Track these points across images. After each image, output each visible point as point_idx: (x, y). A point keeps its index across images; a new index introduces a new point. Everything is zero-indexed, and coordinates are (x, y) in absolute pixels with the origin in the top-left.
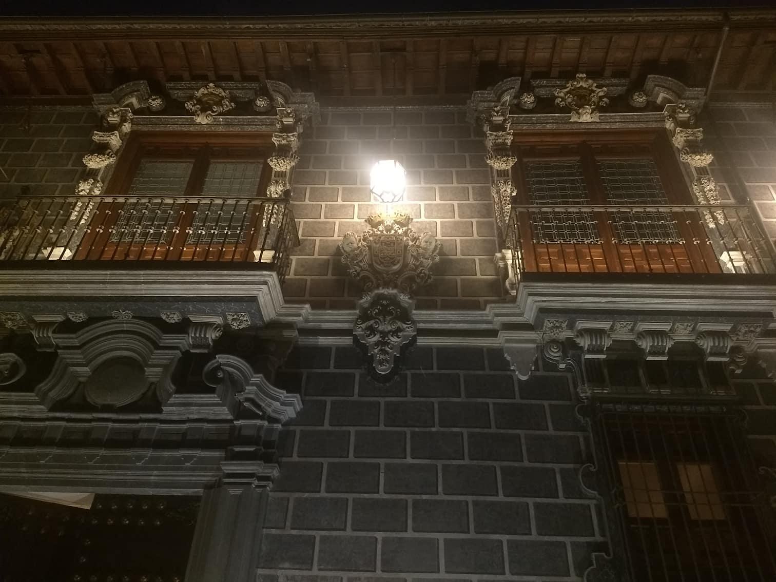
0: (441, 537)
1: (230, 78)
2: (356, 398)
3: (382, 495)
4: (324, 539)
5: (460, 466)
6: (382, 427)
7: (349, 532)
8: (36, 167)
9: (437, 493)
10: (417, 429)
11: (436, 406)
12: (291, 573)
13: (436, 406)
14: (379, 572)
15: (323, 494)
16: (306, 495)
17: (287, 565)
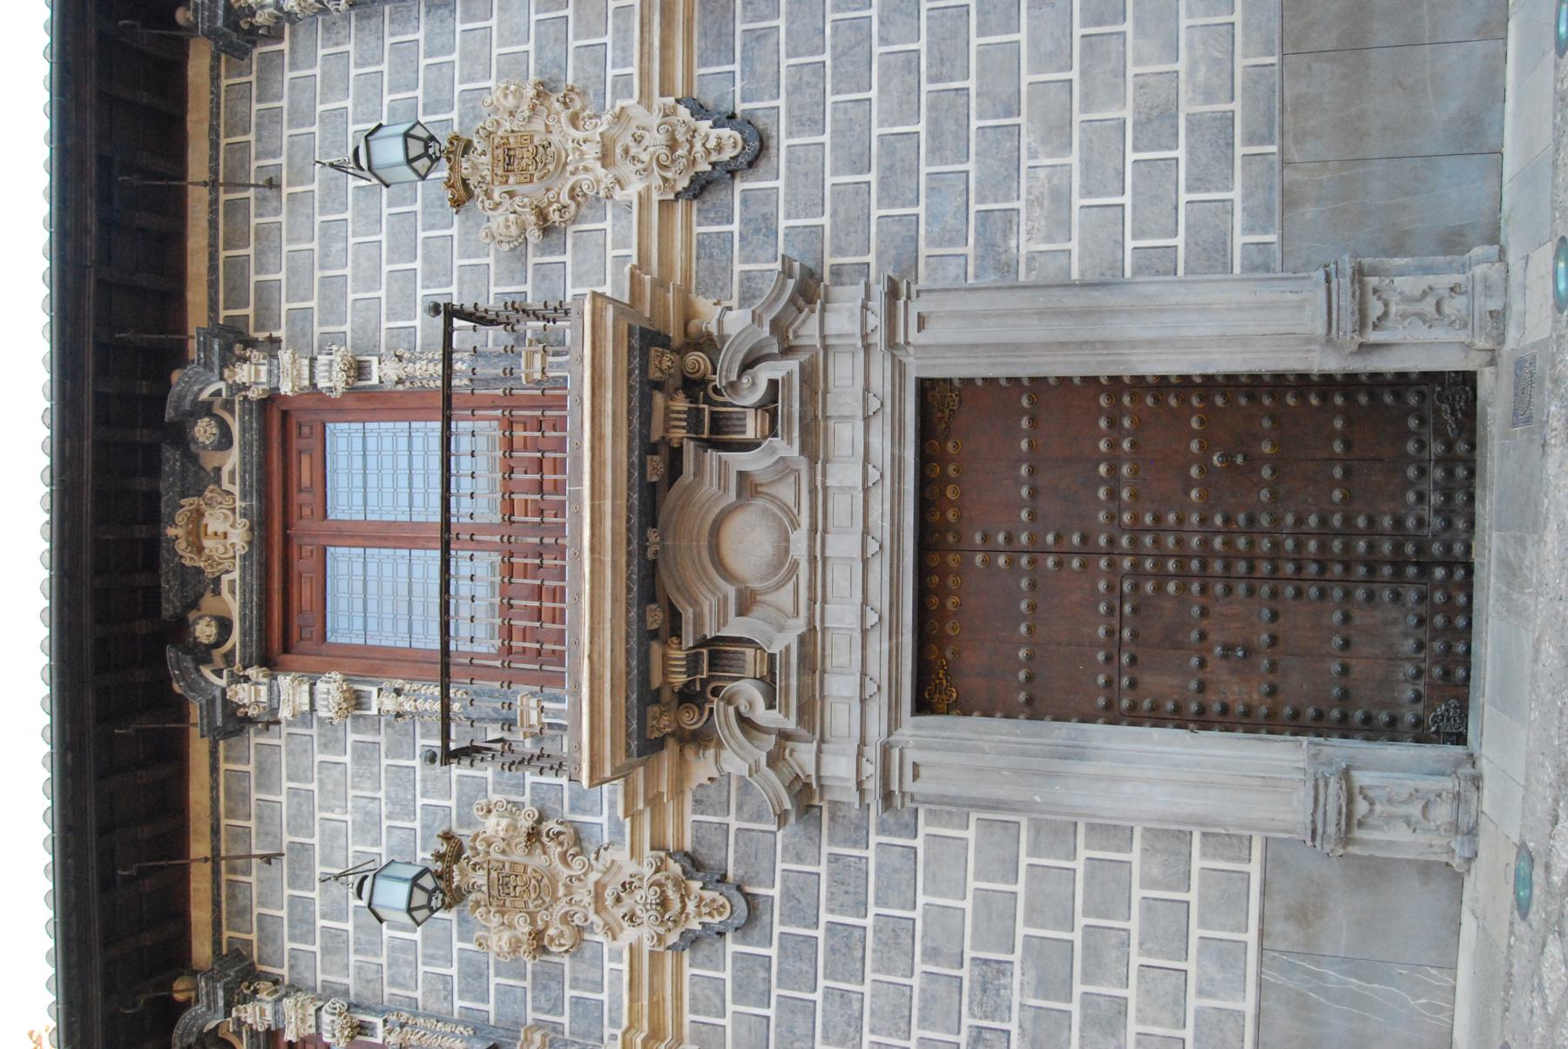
0: (975, 41)
1: (154, 497)
2: (780, 184)
3: (922, 128)
4: (982, 199)
5: (881, 23)
6: (826, 138)
7: (971, 166)
8: (348, 818)
9: (917, 51)
10: (828, 87)
11: (793, 61)
12: (1023, 236)
13: (793, 61)
14: (1022, 120)
15: (921, 210)
16: (922, 232)
17: (1013, 243)
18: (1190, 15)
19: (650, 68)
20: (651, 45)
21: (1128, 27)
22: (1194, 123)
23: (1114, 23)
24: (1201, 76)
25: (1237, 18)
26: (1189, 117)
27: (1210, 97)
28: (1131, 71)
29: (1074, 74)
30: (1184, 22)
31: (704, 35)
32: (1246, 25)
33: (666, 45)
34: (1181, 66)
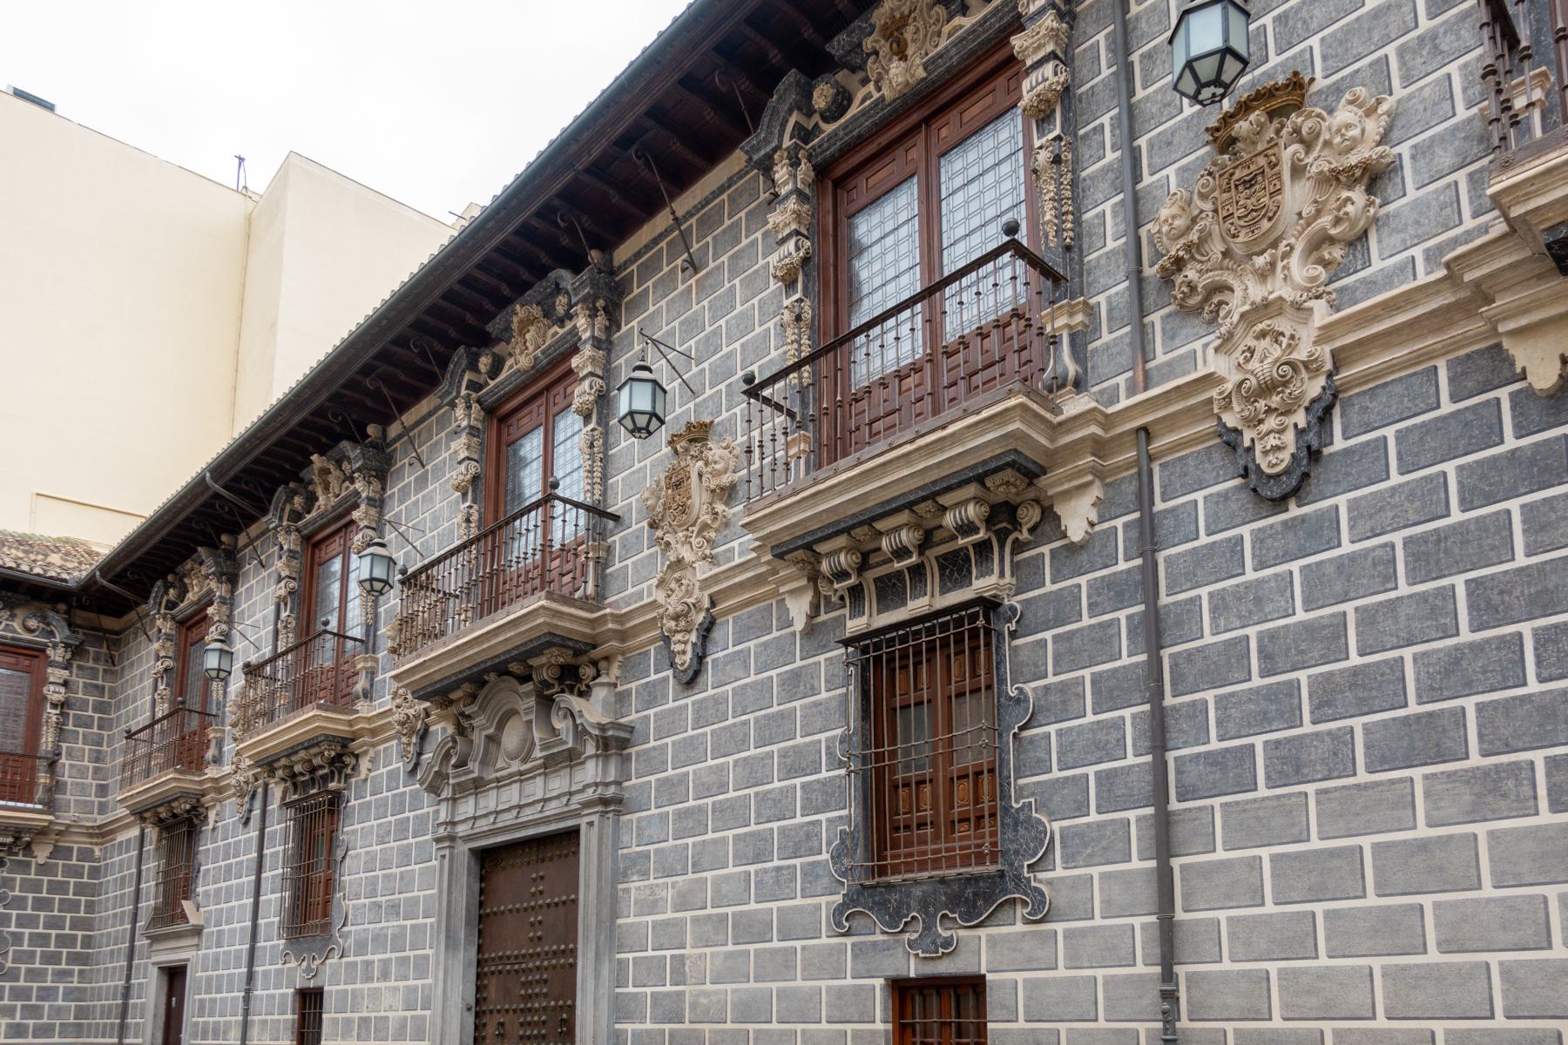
18: (734, 991)
19: (720, 581)
20: (735, 576)
21: (731, 947)
22: (681, 994)
23: (734, 937)
24: (704, 1001)
25: (729, 1026)
26: (683, 993)
27: (694, 1006)
28: (708, 950)
29: (709, 911)
30: (729, 987)
31: (750, 615)
32: (724, 1031)
33: (742, 586)
34: (709, 987)
